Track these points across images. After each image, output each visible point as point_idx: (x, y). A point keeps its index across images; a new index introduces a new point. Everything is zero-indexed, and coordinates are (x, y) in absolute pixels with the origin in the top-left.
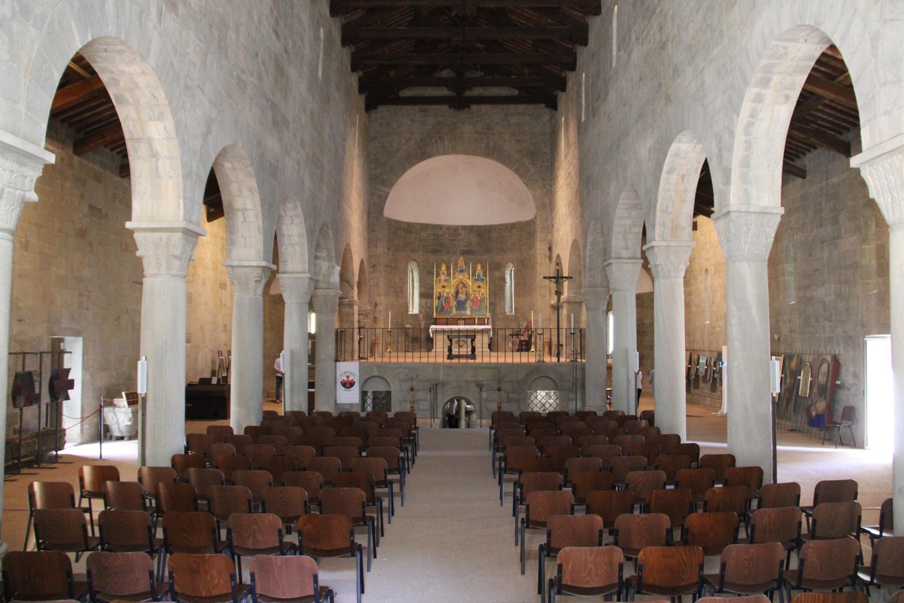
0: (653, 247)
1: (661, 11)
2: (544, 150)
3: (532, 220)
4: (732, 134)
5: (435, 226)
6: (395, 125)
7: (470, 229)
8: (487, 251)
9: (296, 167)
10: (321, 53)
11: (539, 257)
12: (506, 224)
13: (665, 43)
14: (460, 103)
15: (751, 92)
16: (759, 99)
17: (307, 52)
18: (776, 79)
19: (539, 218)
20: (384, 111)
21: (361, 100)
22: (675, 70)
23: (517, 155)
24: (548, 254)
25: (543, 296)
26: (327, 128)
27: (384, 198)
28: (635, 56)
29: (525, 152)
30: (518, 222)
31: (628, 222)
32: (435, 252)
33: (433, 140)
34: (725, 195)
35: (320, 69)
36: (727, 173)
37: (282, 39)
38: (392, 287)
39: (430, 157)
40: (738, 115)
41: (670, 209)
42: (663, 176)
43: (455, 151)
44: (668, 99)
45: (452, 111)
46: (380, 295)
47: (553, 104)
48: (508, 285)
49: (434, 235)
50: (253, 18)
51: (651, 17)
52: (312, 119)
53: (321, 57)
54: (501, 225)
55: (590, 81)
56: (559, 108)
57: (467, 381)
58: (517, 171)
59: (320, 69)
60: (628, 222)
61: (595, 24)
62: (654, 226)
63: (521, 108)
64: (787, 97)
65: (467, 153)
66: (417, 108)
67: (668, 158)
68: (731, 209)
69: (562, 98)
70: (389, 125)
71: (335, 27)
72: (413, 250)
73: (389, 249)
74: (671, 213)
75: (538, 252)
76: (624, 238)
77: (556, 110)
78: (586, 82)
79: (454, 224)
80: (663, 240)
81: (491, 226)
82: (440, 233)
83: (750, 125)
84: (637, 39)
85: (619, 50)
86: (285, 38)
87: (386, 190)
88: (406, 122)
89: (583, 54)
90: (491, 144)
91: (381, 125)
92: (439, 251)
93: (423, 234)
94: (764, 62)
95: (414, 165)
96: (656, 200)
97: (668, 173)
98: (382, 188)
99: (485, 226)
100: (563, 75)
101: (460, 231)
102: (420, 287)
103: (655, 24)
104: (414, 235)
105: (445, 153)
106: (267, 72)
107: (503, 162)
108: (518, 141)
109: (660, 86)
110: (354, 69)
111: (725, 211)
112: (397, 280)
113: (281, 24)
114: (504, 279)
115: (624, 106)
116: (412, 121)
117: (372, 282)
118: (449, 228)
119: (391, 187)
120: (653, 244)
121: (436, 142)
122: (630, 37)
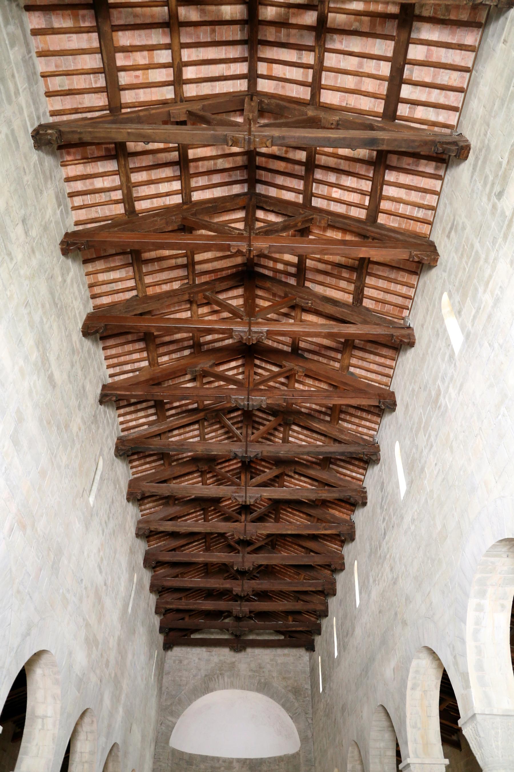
0: (408, 765)
1: (390, 556)
2: (306, 687)
4: (463, 641)
5: (213, 759)
6: (185, 662)
9: (99, 683)
10: (133, 592)
12: (275, 757)
13: (396, 579)
14: (238, 644)
15: (472, 603)
16: (480, 608)
17: (122, 588)
18: (490, 591)
20: (178, 651)
21: (161, 638)
22: (407, 599)
23: (283, 691)
26: (130, 656)
27: (171, 728)
28: (374, 595)
29: (290, 688)
31: (382, 745)
33: (216, 676)
34: (468, 698)
35: (131, 605)
36: (465, 677)
37: (104, 574)
39: (212, 691)
40: (465, 623)
41: (419, 725)
42: (409, 692)
43: (232, 686)
44: (405, 623)
45: (232, 653)
47: (310, 647)
49: (212, 767)
50: (83, 553)
51: (383, 563)
52: (119, 645)
53: (133, 595)
54: (270, 758)
55: (340, 622)
56: (316, 649)
58: (283, 706)
59: (131, 605)
60: (382, 745)
61: (340, 578)
62: (406, 743)
63: (286, 651)
64: (503, 606)
65: (242, 688)
66: (204, 649)
67: (411, 675)
68: (476, 712)
69: (318, 640)
70: (181, 662)
71: (147, 576)
74: (419, 729)
76: (381, 762)
77: (314, 651)
78: (337, 624)
80: (417, 757)
81: (262, 759)
82: (217, 765)
83: (476, 632)
84: (374, 581)
85: (360, 593)
86: (106, 574)
87: (174, 720)
88: (194, 659)
89: (333, 603)
90: (263, 680)
91: (174, 662)
93: (202, 766)
94: (478, 576)
95: (199, 697)
96: (405, 716)
97: (412, 689)
98: (170, 718)
99: (257, 759)
100: (318, 622)
101: (235, 764)
103: (387, 566)
104: (194, 767)
105: (224, 688)
106: (88, 597)
107: (272, 697)
108: (284, 678)
109: (396, 614)
110: (157, 612)
111: (470, 714)
113: (105, 562)
115: (369, 636)
116: (199, 659)
118: (225, 760)
119: (178, 718)
120: (409, 761)
121: (218, 677)
122: (368, 582)
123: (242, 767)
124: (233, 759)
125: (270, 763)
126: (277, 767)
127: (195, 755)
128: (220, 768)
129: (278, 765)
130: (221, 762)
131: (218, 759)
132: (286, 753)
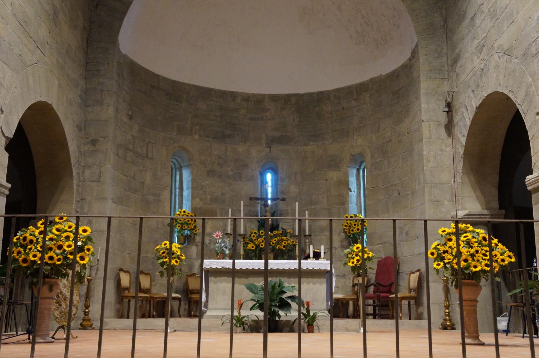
5: (223, 94)
11: (425, 126)
12: (349, 87)
19: (422, 52)
24: (443, 118)
25: (437, 203)
30: (371, 80)
32: (221, 137)
38: (136, 191)
46: (104, 199)
48: (353, 195)
54: (338, 90)
73: (131, 118)
79: (256, 92)
81: (322, 93)
99: (310, 95)
102: (193, 197)
112: (148, 178)
114: (346, 184)
117: (87, 173)
118: (247, 98)
124: (264, 95)
126: (354, 103)
127: (185, 84)
129: (355, 99)
130: (239, 100)
131: (233, 95)
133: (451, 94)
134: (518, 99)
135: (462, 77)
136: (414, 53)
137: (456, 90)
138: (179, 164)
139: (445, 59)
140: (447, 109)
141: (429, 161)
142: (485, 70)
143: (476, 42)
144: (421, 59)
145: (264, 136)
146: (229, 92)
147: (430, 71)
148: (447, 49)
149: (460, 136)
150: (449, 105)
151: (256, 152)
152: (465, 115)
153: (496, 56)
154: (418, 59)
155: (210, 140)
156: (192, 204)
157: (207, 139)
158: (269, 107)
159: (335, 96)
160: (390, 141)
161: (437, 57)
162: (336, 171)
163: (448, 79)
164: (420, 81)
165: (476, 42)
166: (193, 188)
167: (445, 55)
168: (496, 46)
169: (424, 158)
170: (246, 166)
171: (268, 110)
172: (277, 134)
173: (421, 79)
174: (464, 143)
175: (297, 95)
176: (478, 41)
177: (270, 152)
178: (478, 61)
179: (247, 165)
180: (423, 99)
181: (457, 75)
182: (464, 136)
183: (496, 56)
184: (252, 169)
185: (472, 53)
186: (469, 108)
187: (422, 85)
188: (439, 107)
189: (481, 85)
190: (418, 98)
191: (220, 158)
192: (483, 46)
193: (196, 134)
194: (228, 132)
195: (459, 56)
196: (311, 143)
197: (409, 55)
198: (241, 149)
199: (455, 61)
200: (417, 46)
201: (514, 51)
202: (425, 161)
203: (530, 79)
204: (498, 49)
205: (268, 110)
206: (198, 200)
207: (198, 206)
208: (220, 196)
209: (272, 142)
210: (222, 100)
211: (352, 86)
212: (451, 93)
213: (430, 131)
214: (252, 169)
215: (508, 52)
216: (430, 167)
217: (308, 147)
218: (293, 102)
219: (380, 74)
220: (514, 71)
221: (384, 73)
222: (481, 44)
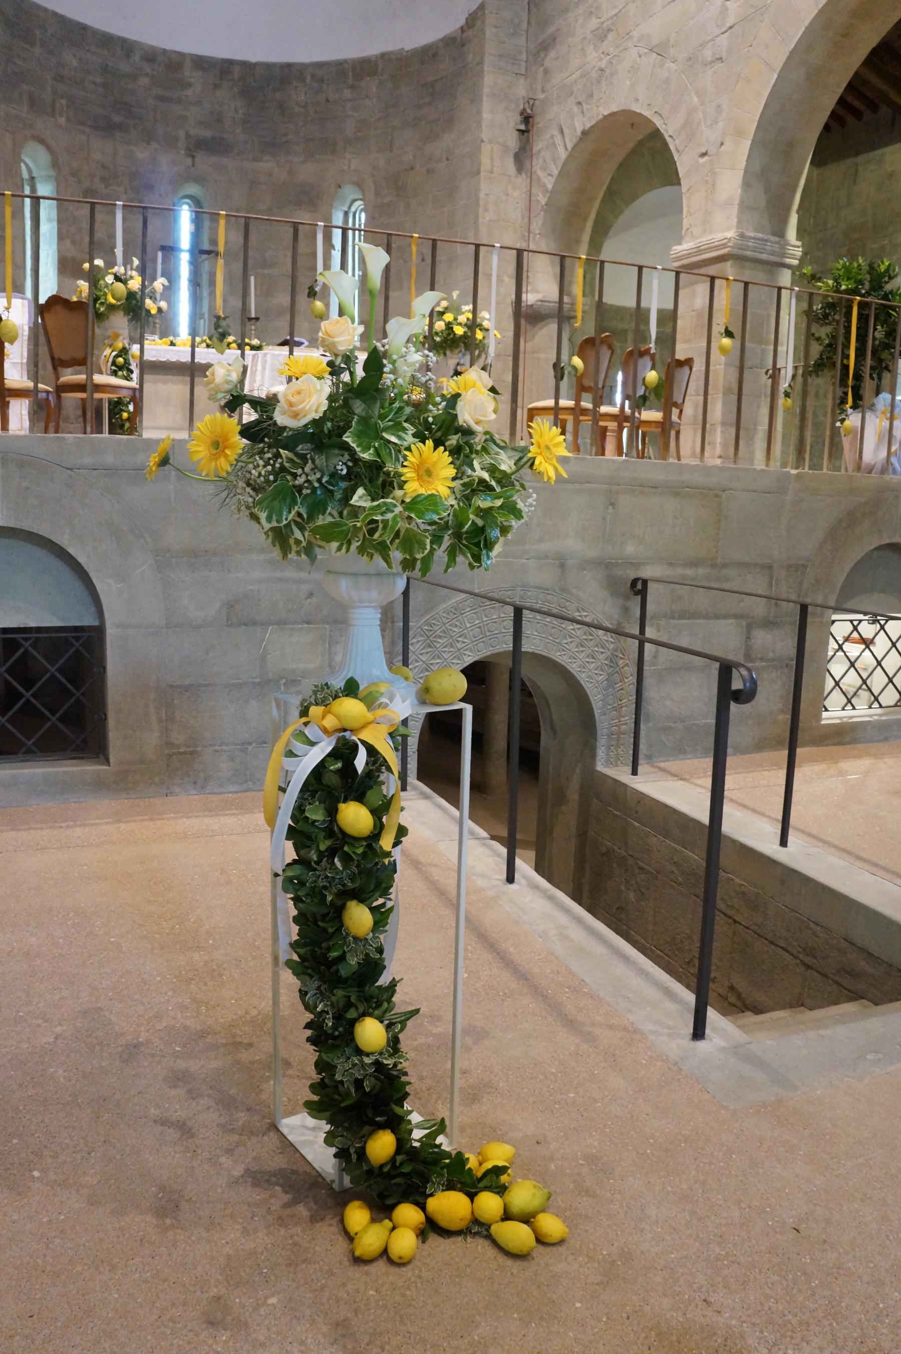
3: (449, 41)
5: (107, 41)
7: (223, 70)
8: (274, 146)
11: (486, 149)
12: (340, 64)
24: (513, 141)
30: (383, 55)
32: (107, 128)
49: (105, 69)
54: (320, 65)
57: (561, 563)
72: (34, 104)
75: (485, 134)
79: (169, 46)
81: (289, 65)
82: (124, 67)
92: (120, 127)
93: (70, 58)
99: (268, 66)
101: (188, 73)
102: (61, 238)
118: (152, 56)
123: (216, 86)
124: (182, 55)
125: (322, 81)
126: (347, 93)
128: (134, 77)
129: (352, 87)
130: (136, 57)
131: (127, 47)
132: (389, 47)
133: (531, 102)
134: (669, 129)
135: (557, 79)
136: (473, 20)
137: (542, 96)
138: (29, 170)
139: (522, 41)
140: (523, 127)
141: (486, 210)
142: (608, 72)
143: (594, 23)
144: (489, 32)
145: (182, 134)
146: (119, 38)
147: (500, 56)
148: (529, 23)
149: (540, 173)
150: (527, 119)
151: (168, 163)
152: (558, 140)
153: (634, 52)
154: (483, 31)
155: (87, 130)
156: (59, 250)
157: (81, 127)
158: (192, 80)
159: (313, 76)
160: (412, 169)
161: (513, 34)
162: (310, 211)
163: (526, 76)
164: (482, 71)
165: (594, 23)
166: (60, 221)
167: (524, 33)
168: (635, 34)
169: (481, 203)
170: (150, 187)
171: (190, 85)
172: (207, 133)
173: (486, 68)
174: (550, 187)
175: (245, 65)
176: (599, 20)
177: (193, 165)
178: (595, 54)
179: (152, 187)
180: (486, 104)
181: (546, 72)
182: (550, 175)
183: (634, 52)
184: (160, 195)
185: (585, 38)
186: (566, 131)
187: (486, 79)
188: (508, 122)
189: (596, 96)
190: (476, 100)
191: (104, 167)
192: (609, 30)
193: (61, 116)
194: (117, 119)
195: (554, 39)
196: (267, 157)
197: (462, 22)
198: (142, 154)
199: (545, 47)
200: (482, 7)
201: (672, 51)
202: (481, 209)
203: (695, 99)
204: (639, 41)
205: (190, 85)
206: (68, 242)
207: (69, 255)
208: (106, 238)
209: (197, 146)
210: (106, 52)
211: (345, 61)
212: (531, 101)
213: (492, 159)
214: (160, 195)
215: (660, 50)
216: (488, 218)
217: (261, 164)
218: (236, 76)
219: (400, 47)
220: (667, 81)
221: (408, 47)
222: (605, 25)
